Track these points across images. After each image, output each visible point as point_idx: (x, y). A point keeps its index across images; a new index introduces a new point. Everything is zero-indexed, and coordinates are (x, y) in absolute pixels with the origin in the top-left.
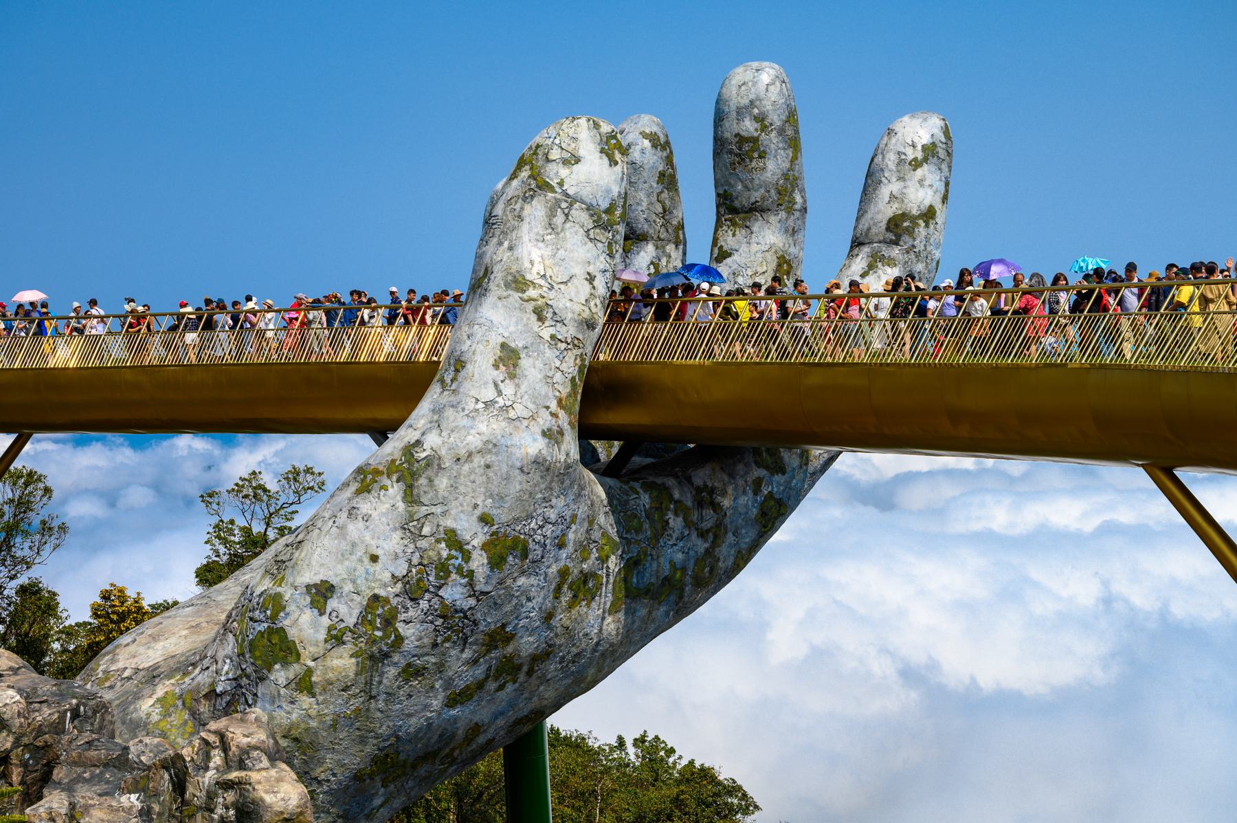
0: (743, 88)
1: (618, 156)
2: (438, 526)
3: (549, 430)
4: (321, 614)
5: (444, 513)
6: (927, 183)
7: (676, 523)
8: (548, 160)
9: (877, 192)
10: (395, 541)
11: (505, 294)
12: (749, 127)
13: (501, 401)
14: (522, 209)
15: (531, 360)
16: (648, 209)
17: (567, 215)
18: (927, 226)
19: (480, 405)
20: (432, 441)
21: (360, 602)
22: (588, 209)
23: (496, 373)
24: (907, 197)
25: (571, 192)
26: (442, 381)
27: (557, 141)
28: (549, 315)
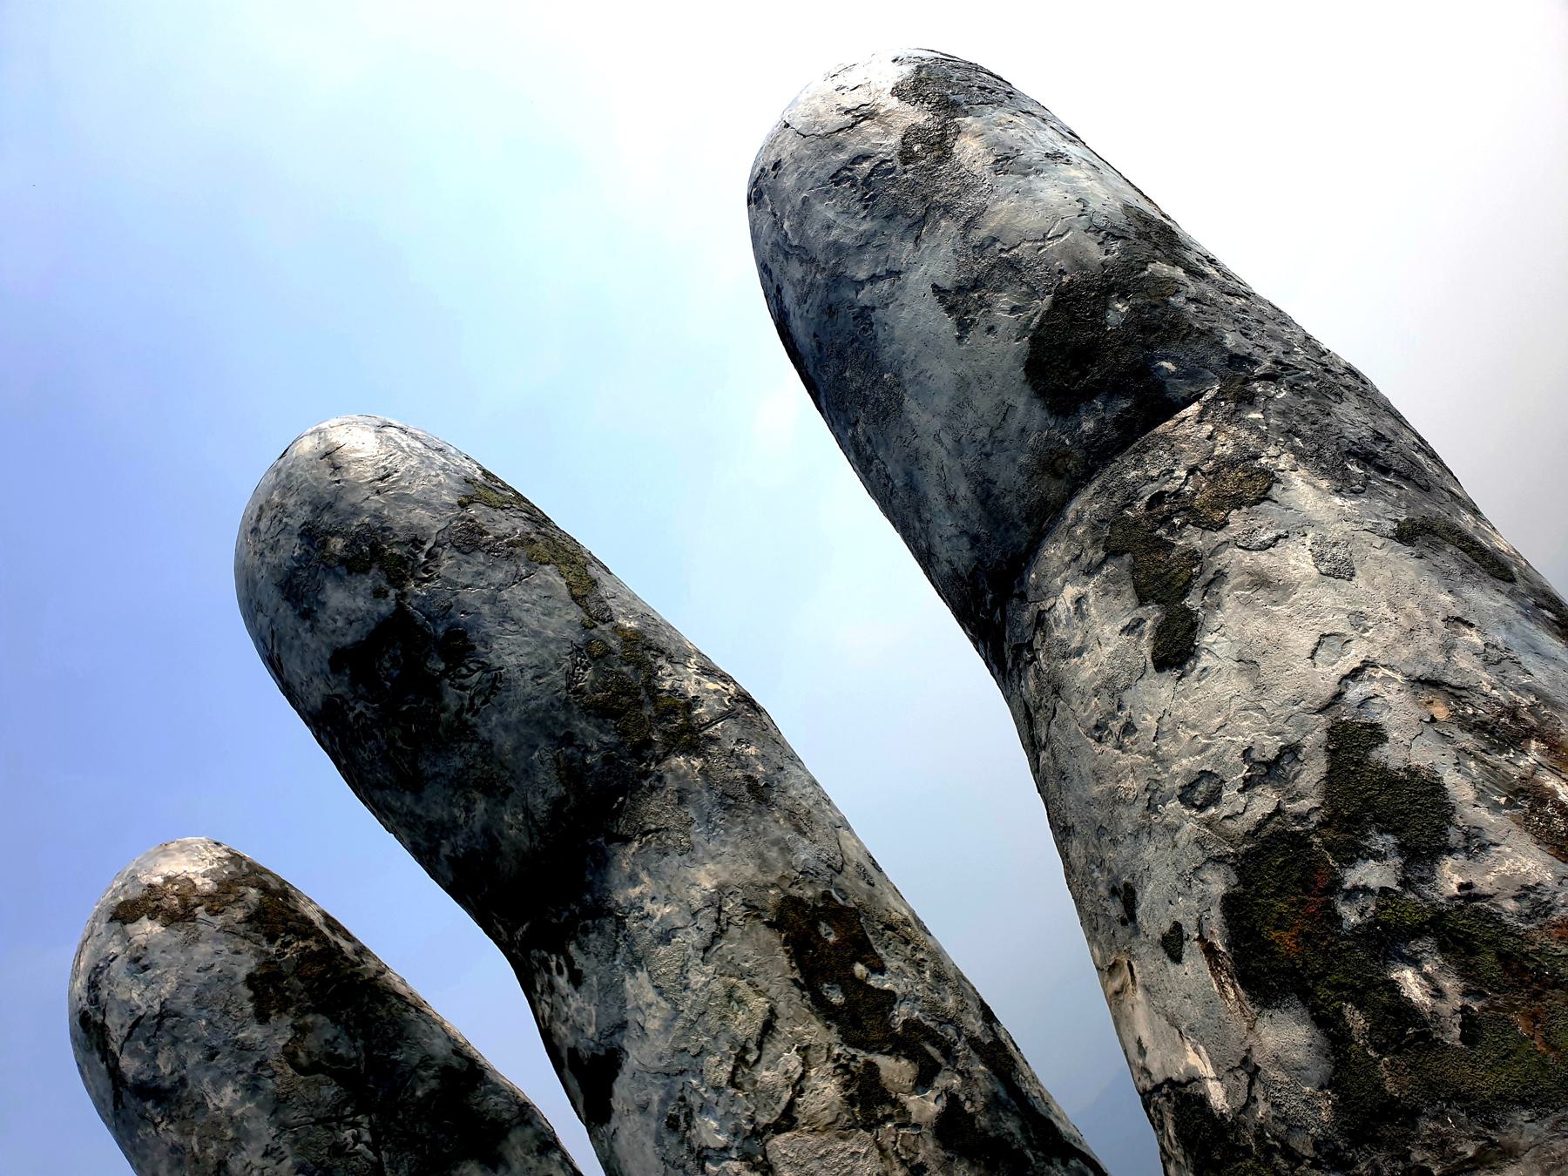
0: (263, 526)
9: (887, 354)
12: (349, 603)
16: (283, 1127)
24: (1013, 237)
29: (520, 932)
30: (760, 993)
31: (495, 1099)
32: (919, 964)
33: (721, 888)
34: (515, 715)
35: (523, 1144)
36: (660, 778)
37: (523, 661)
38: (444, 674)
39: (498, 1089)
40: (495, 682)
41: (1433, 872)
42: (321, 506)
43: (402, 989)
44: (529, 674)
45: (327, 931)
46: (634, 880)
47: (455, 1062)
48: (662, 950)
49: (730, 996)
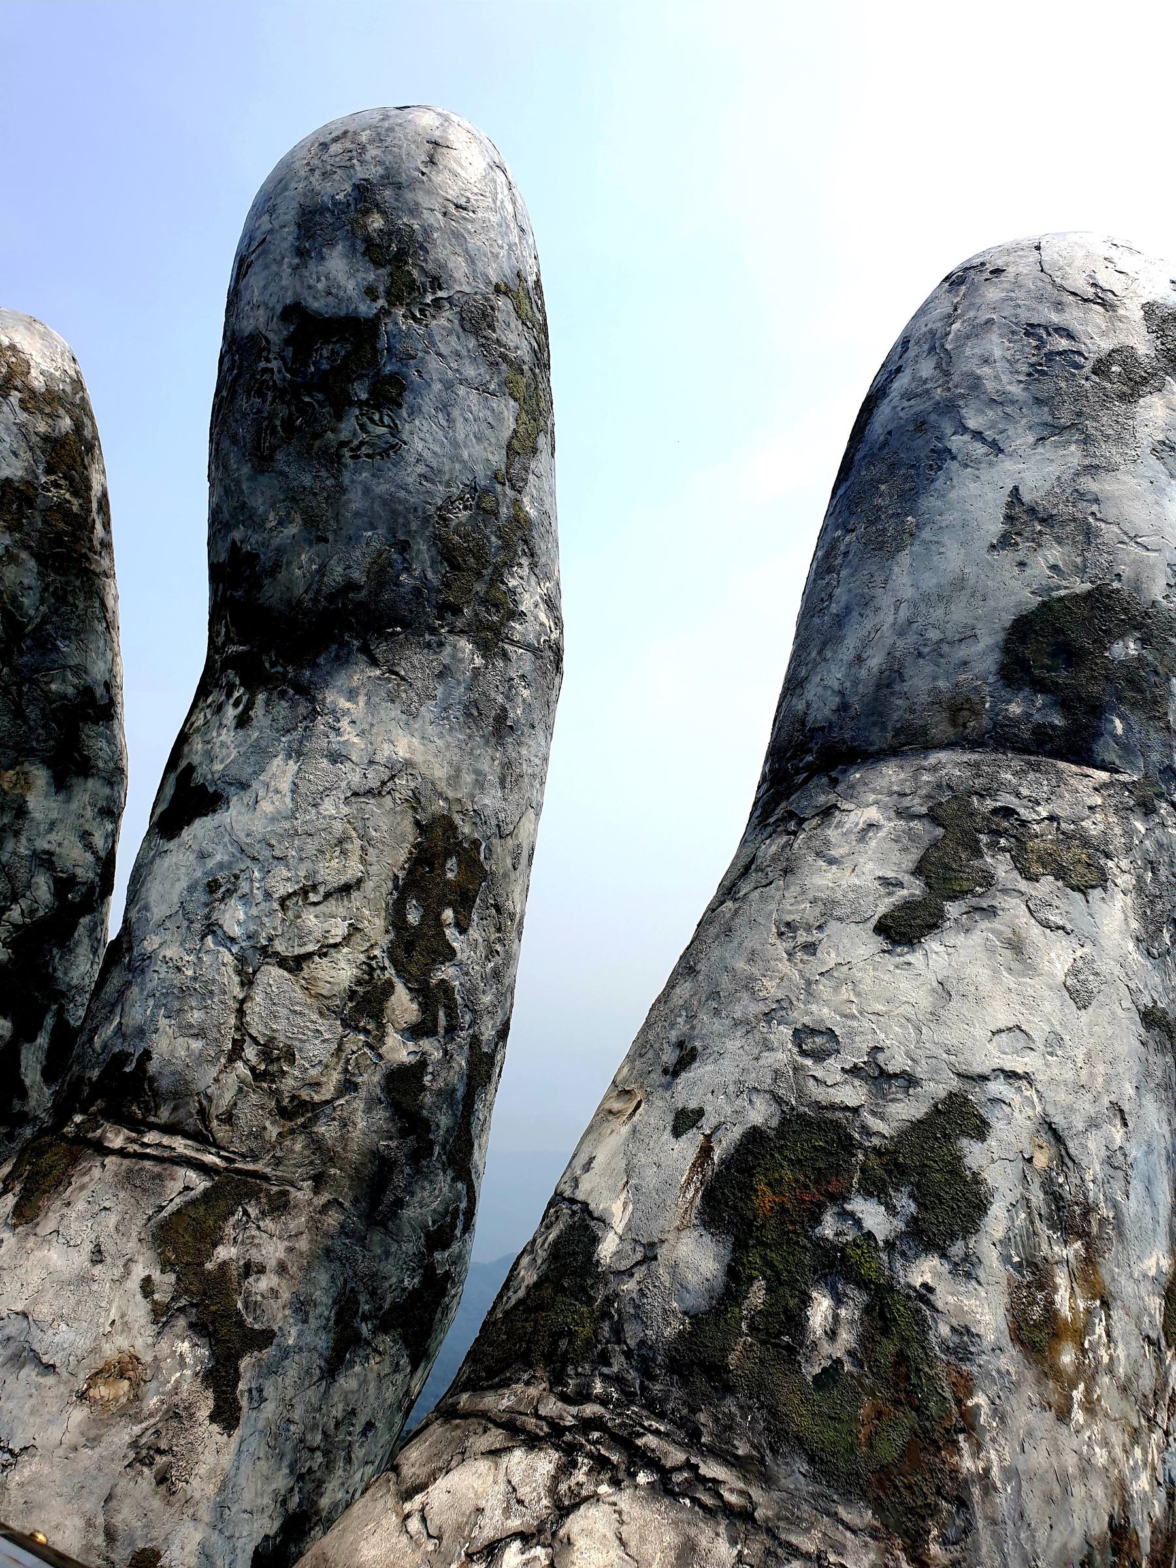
0: (335, 148)
9: (928, 503)
12: (342, 278)
24: (1110, 512)
29: (233, 649)
30: (363, 861)
31: (103, 744)
32: (491, 953)
33: (408, 764)
34: (381, 488)
35: (94, 794)
36: (441, 644)
37: (427, 454)
38: (361, 404)
39: (111, 740)
40: (391, 449)
41: (917, 1256)
42: (392, 179)
43: (110, 602)
44: (421, 469)
45: (95, 506)
46: (352, 695)
47: (100, 691)
48: (324, 763)
49: (340, 842)
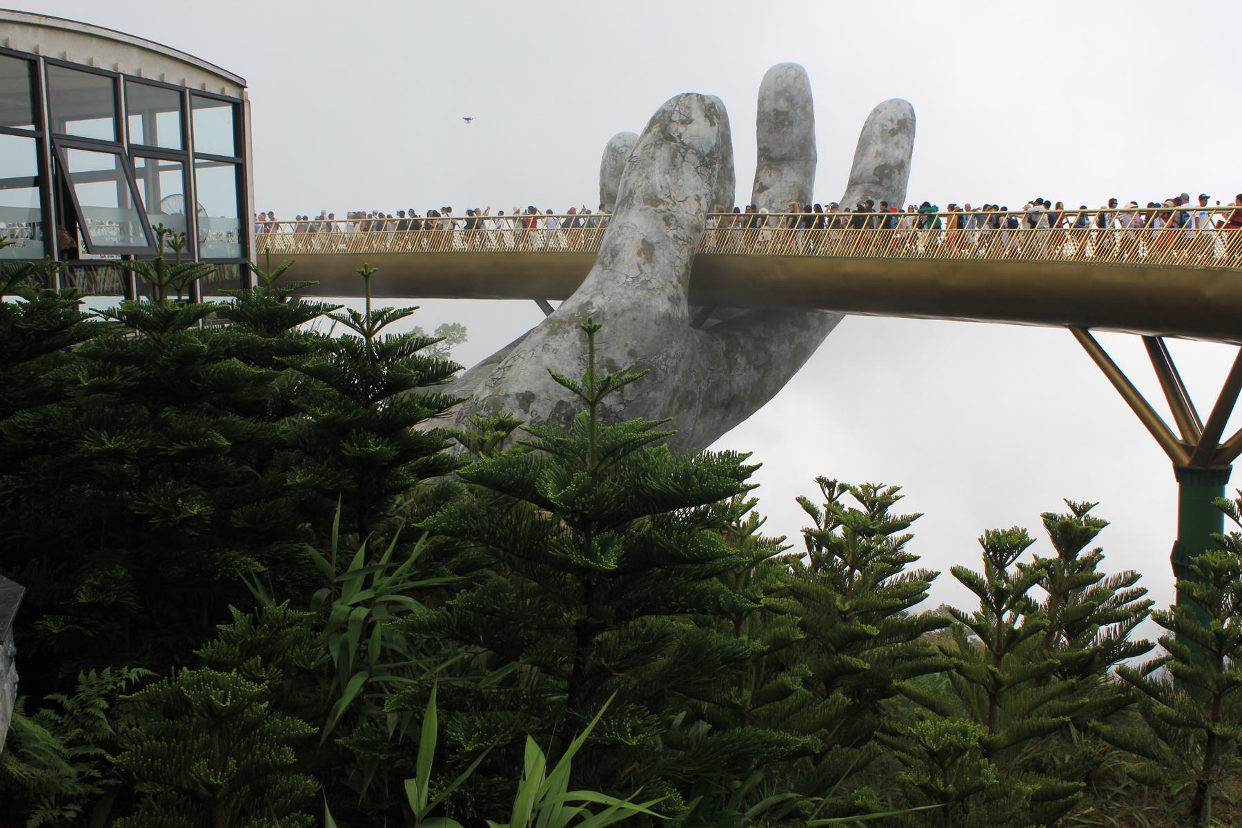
1: (716, 120)
2: (602, 357)
3: (672, 296)
4: (526, 412)
5: (607, 349)
6: (900, 145)
7: (742, 361)
8: (671, 121)
10: (574, 367)
11: (644, 207)
13: (643, 278)
14: (654, 152)
15: (661, 251)
17: (684, 157)
18: (900, 173)
19: (630, 280)
20: (598, 302)
21: (551, 405)
22: (697, 154)
23: (639, 259)
25: (686, 142)
26: (602, 263)
27: (677, 109)
28: (673, 222)
40: (792, 132)
